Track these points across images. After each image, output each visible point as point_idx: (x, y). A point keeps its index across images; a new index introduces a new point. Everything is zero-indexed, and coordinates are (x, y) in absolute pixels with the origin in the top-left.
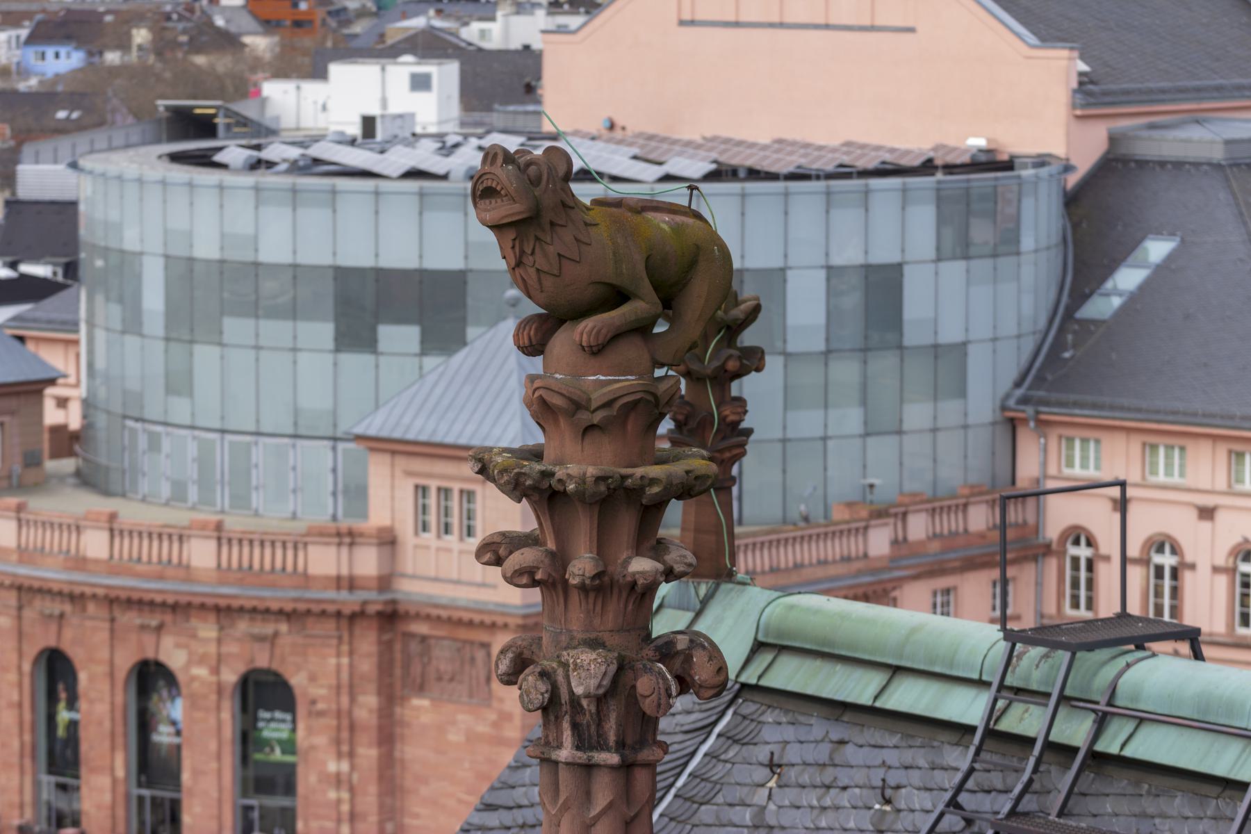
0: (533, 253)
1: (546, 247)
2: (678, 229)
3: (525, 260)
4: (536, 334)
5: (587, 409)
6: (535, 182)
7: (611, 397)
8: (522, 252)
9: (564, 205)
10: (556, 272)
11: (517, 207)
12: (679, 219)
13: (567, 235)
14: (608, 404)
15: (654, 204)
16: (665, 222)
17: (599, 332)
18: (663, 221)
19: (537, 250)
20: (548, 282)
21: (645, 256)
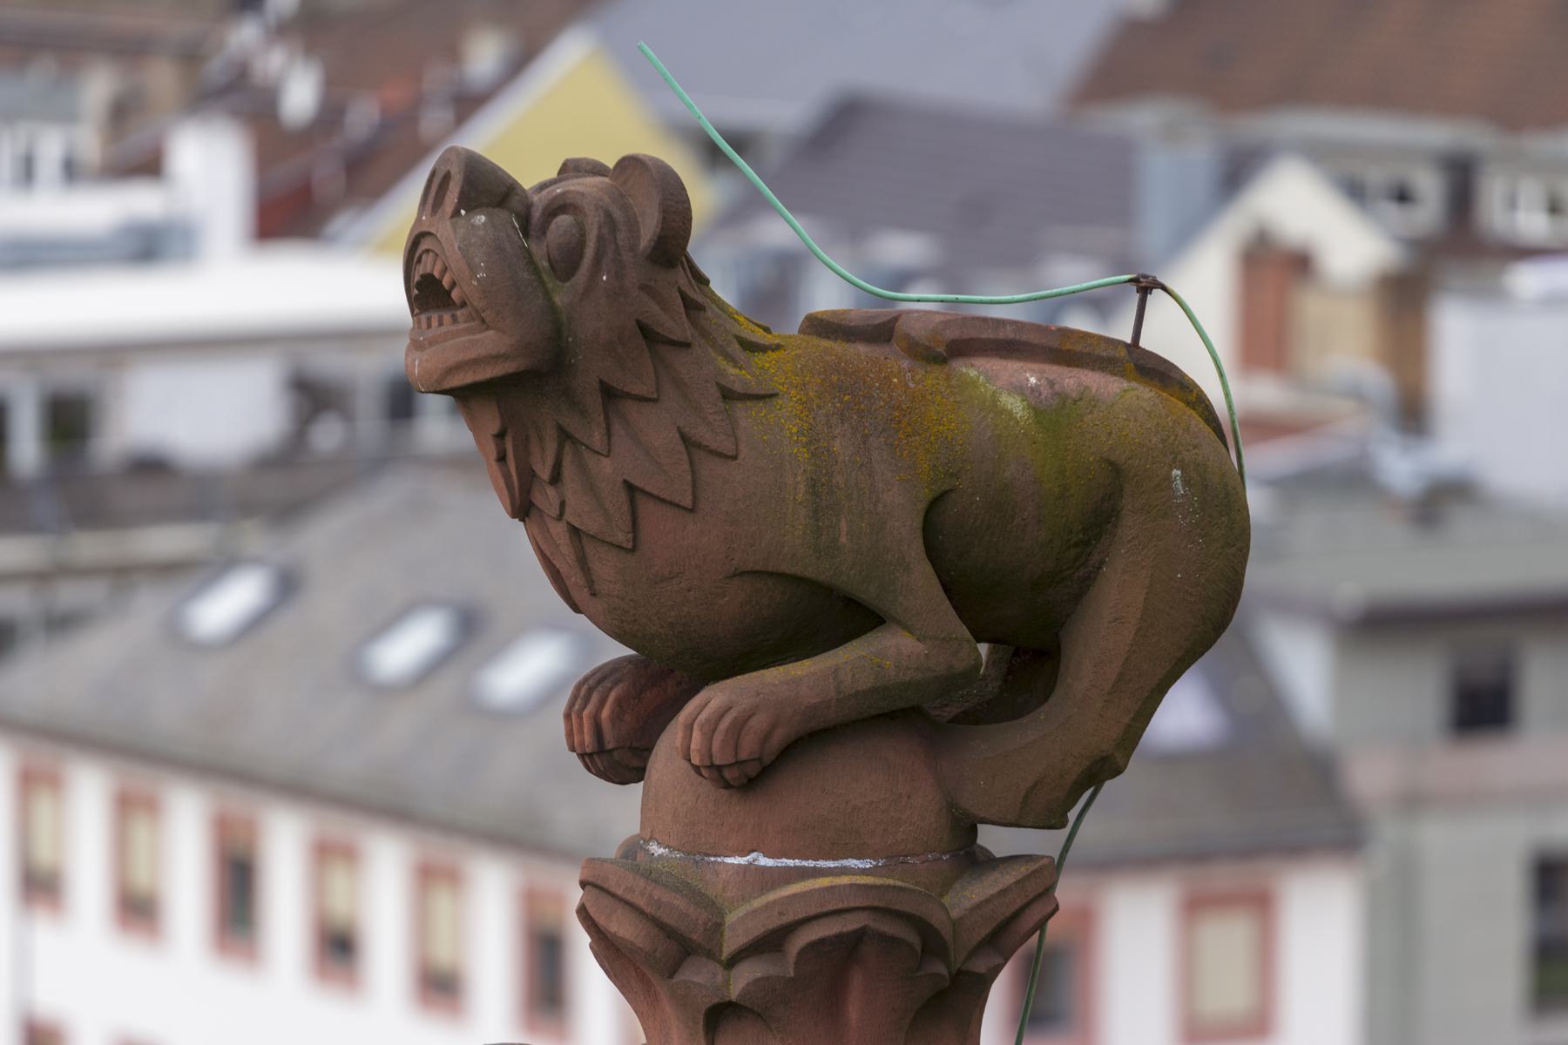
0: (556, 479)
1: (591, 460)
2: (1054, 414)
3: (538, 499)
4: (616, 717)
5: (711, 955)
6: (567, 263)
7: (774, 922)
8: (528, 477)
9: (648, 334)
10: (622, 537)
11: (489, 341)
12: (1072, 379)
13: (657, 427)
14: (769, 943)
15: (1009, 334)
16: (1020, 390)
17: (739, 726)
18: (1012, 387)
19: (568, 470)
20: (605, 566)
21: (926, 495)
